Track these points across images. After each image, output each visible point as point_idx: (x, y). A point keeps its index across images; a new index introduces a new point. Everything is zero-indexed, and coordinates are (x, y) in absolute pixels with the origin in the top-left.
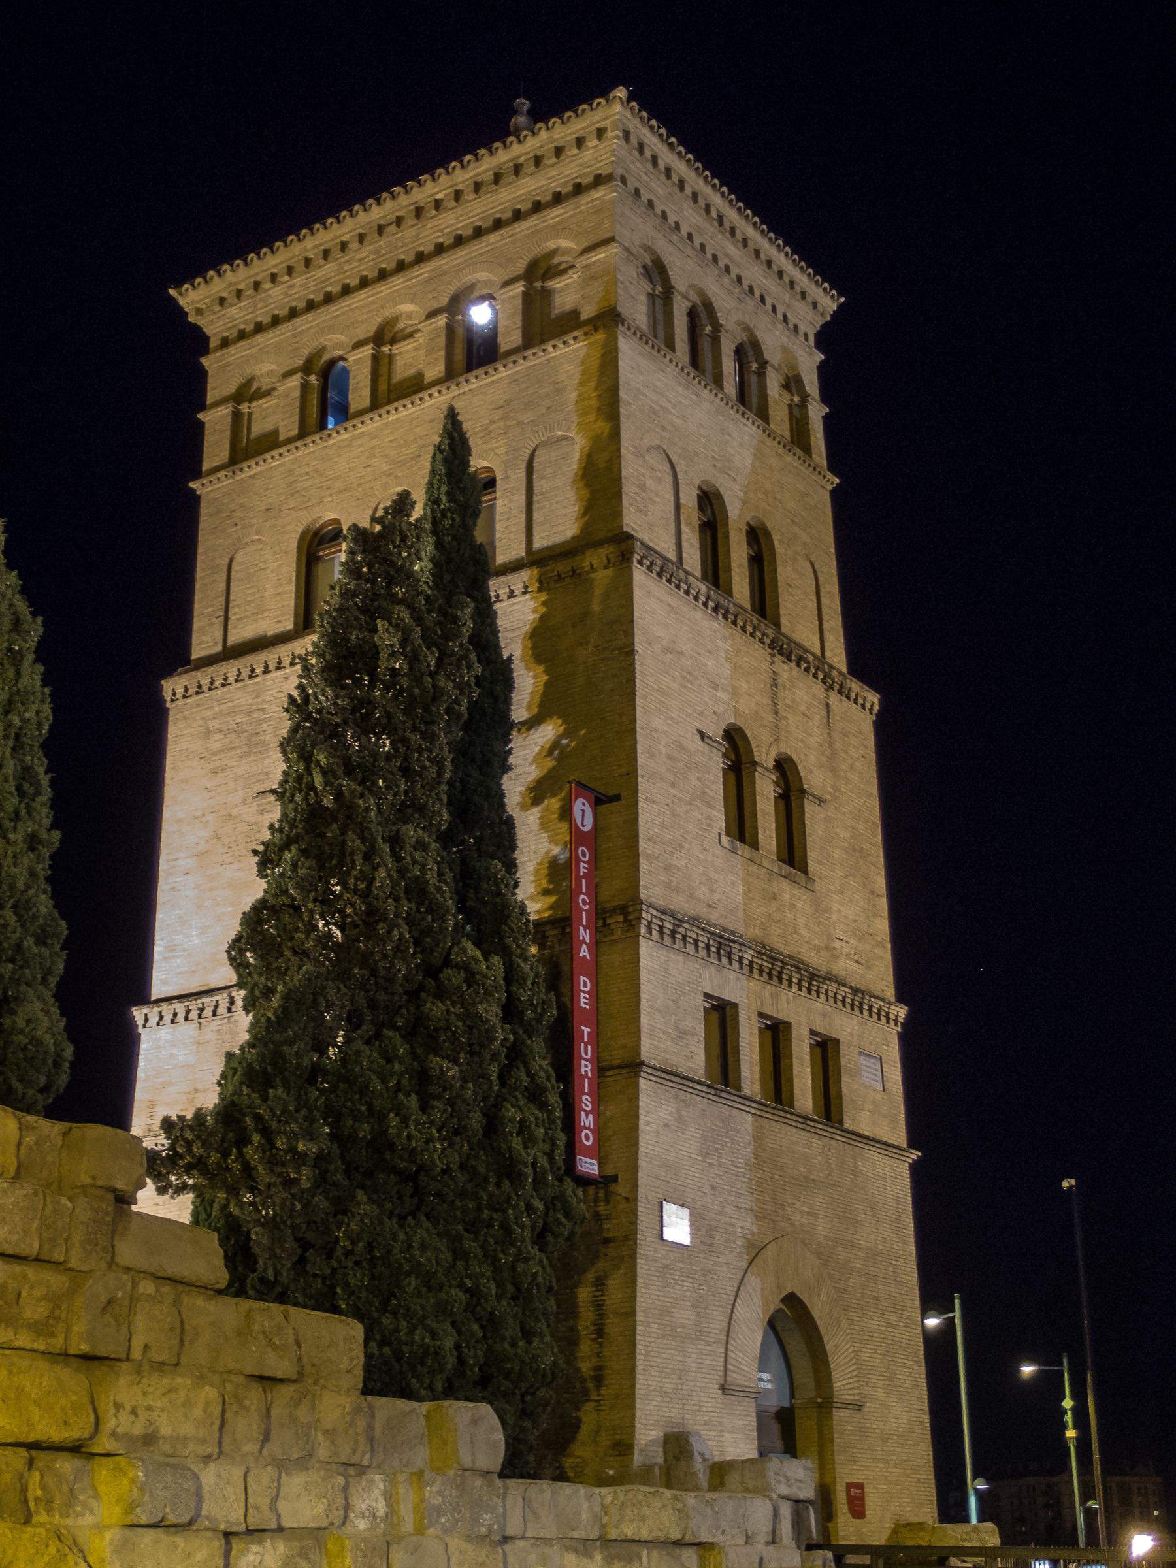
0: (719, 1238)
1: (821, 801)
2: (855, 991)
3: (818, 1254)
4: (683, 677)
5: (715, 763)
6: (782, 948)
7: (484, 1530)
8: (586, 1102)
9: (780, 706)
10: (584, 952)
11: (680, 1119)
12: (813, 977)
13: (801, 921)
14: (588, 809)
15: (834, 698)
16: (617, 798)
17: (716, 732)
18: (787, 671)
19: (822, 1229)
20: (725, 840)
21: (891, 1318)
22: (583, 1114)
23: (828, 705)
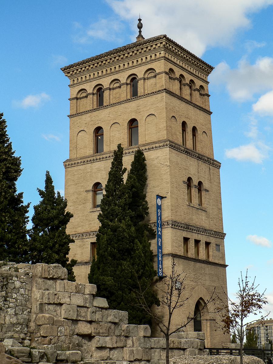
1: (208, 191)
2: (215, 232)
3: (206, 289)
4: (179, 169)
5: (185, 187)
7: (148, 347)
12: (206, 230)
13: (203, 218)
14: (160, 200)
15: (211, 167)
16: (166, 197)
17: (186, 180)
19: (208, 283)
23: (210, 168)
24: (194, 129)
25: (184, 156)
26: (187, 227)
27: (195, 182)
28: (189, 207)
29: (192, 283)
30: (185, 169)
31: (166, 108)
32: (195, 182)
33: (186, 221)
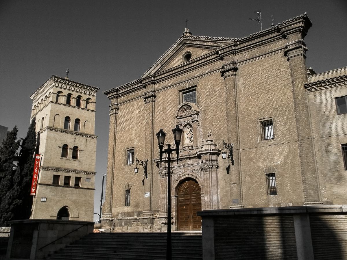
0: (52, 201)
2: (85, 172)
6: (71, 168)
8: (34, 187)
9: (76, 140)
10: (36, 172)
11: (46, 188)
12: (76, 171)
13: (76, 165)
15: (88, 138)
17: (62, 146)
18: (77, 136)
19: (74, 198)
20: (61, 157)
21: (87, 208)
22: (33, 189)
23: (87, 139)
24: (77, 121)
25: (62, 134)
26: (58, 169)
27: (71, 146)
28: (62, 159)
29: (58, 198)
30: (62, 140)
31: (51, 111)
32: (71, 146)
33: (57, 166)
